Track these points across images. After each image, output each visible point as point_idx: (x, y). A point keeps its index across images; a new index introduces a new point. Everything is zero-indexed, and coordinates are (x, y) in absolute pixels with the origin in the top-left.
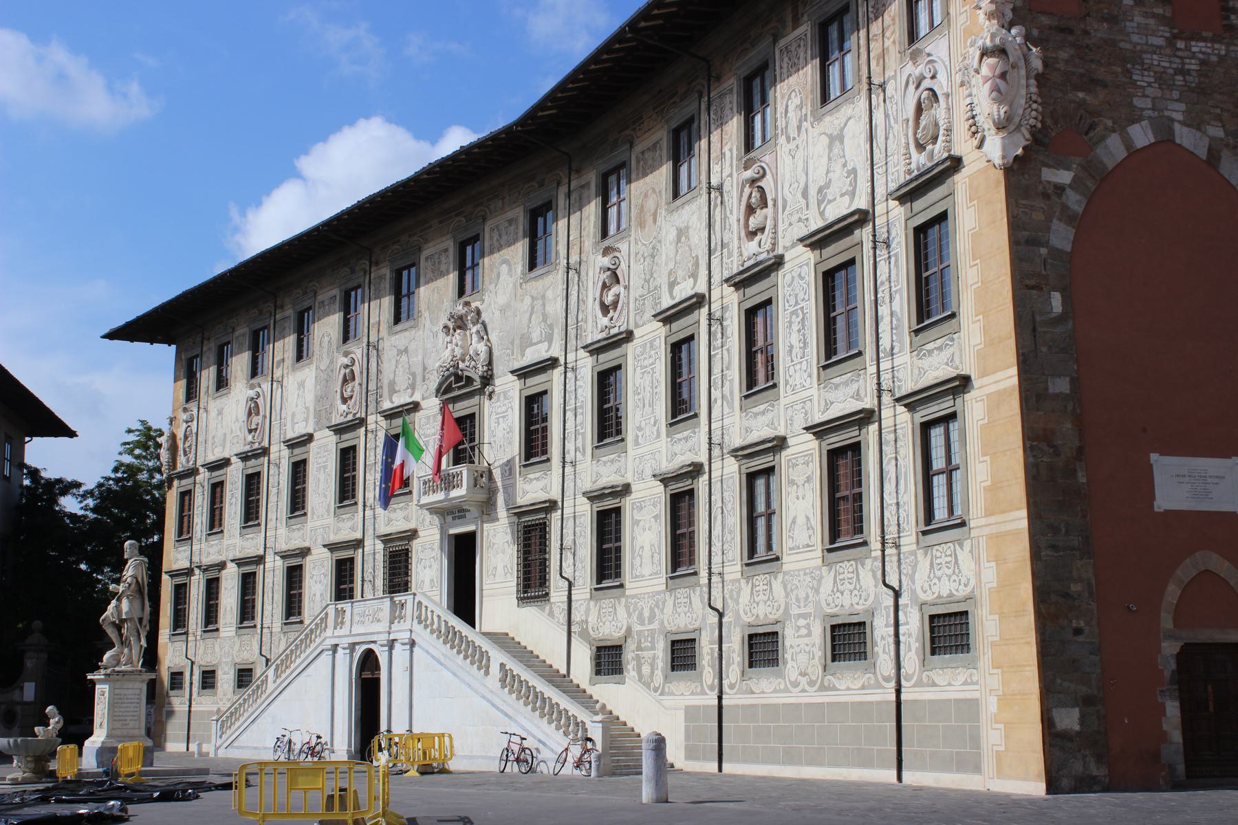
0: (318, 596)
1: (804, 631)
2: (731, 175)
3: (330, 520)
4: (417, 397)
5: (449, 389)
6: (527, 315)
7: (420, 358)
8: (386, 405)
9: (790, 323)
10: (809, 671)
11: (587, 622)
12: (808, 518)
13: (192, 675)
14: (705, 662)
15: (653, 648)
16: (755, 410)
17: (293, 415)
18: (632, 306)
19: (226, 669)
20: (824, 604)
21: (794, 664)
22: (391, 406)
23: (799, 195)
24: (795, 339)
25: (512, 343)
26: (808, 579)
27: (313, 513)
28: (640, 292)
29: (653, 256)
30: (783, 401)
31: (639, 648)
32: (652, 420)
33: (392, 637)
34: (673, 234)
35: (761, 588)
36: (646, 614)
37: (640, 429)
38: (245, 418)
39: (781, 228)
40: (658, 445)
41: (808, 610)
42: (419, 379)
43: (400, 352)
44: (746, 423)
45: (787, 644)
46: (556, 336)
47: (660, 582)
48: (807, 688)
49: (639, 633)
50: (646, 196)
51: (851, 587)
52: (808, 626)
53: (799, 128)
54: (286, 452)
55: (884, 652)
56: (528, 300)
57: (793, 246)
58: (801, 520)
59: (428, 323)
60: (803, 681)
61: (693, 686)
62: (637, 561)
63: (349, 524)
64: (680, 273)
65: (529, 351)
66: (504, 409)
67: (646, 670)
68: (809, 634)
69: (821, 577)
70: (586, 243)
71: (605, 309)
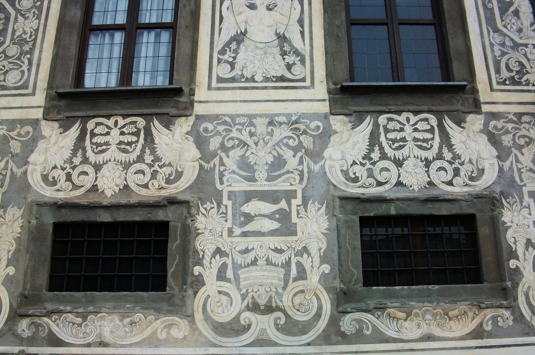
1: (275, 225)
10: (286, 302)
12: (282, 38)
20: (337, 178)
21: (226, 286)
35: (115, 136)
41: (281, 185)
45: (204, 244)
48: (274, 334)
51: (430, 155)
52: (284, 217)
60: (262, 324)
69: (325, 136)
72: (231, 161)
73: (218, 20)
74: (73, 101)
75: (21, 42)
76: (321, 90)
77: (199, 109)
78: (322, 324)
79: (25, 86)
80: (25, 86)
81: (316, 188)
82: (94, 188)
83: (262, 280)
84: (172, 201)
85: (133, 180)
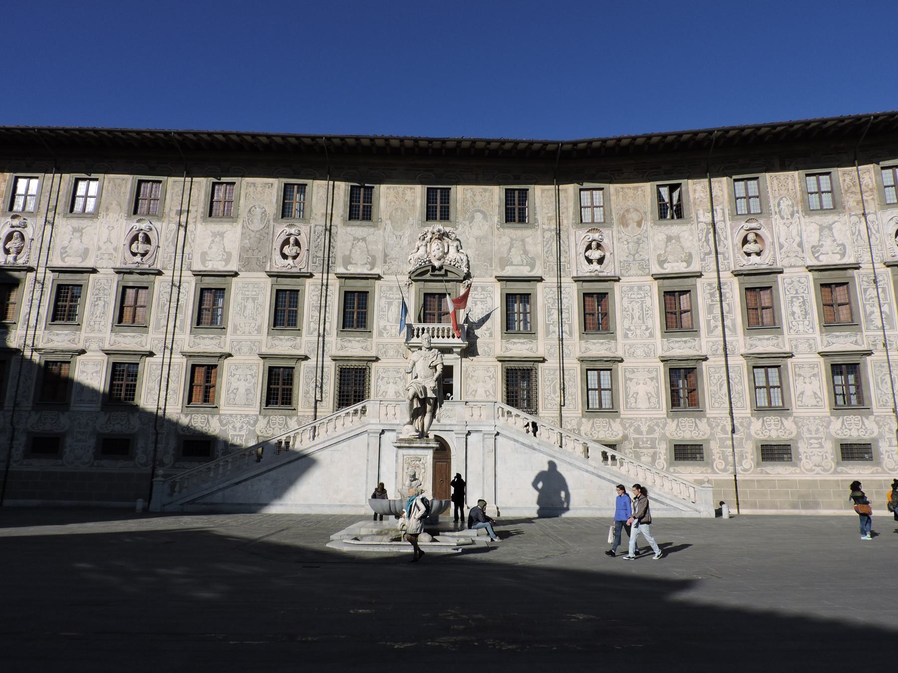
0: (242, 390)
2: (724, 221)
4: (376, 271)
5: (426, 272)
6: (507, 247)
7: (380, 247)
8: (341, 270)
9: (792, 302)
10: (823, 464)
11: (579, 430)
13: (12, 439)
17: (204, 255)
20: (834, 434)
22: (345, 271)
23: (795, 245)
24: (796, 309)
25: (491, 259)
26: (818, 421)
28: (625, 259)
29: (638, 242)
30: (786, 336)
31: (637, 445)
32: (644, 327)
33: (468, 428)
36: (644, 429)
37: (629, 329)
38: (127, 242)
39: (778, 257)
41: (819, 435)
42: (379, 261)
43: (355, 239)
44: (749, 341)
45: (801, 450)
50: (628, 211)
52: (820, 444)
53: (792, 215)
54: (193, 280)
55: (888, 457)
56: (506, 240)
57: (791, 266)
58: (808, 393)
59: (389, 227)
60: (818, 469)
61: (703, 469)
62: (632, 400)
63: (290, 343)
64: (670, 258)
65: (507, 268)
66: (482, 296)
68: (821, 446)
69: (829, 423)
71: (590, 261)
72: (805, 429)
73: (795, 387)
74: (759, 410)
75: (738, 393)
76: (827, 409)
77: (794, 414)
78: (832, 470)
81: (829, 436)
83: (817, 459)
84: (791, 440)
85: (780, 434)
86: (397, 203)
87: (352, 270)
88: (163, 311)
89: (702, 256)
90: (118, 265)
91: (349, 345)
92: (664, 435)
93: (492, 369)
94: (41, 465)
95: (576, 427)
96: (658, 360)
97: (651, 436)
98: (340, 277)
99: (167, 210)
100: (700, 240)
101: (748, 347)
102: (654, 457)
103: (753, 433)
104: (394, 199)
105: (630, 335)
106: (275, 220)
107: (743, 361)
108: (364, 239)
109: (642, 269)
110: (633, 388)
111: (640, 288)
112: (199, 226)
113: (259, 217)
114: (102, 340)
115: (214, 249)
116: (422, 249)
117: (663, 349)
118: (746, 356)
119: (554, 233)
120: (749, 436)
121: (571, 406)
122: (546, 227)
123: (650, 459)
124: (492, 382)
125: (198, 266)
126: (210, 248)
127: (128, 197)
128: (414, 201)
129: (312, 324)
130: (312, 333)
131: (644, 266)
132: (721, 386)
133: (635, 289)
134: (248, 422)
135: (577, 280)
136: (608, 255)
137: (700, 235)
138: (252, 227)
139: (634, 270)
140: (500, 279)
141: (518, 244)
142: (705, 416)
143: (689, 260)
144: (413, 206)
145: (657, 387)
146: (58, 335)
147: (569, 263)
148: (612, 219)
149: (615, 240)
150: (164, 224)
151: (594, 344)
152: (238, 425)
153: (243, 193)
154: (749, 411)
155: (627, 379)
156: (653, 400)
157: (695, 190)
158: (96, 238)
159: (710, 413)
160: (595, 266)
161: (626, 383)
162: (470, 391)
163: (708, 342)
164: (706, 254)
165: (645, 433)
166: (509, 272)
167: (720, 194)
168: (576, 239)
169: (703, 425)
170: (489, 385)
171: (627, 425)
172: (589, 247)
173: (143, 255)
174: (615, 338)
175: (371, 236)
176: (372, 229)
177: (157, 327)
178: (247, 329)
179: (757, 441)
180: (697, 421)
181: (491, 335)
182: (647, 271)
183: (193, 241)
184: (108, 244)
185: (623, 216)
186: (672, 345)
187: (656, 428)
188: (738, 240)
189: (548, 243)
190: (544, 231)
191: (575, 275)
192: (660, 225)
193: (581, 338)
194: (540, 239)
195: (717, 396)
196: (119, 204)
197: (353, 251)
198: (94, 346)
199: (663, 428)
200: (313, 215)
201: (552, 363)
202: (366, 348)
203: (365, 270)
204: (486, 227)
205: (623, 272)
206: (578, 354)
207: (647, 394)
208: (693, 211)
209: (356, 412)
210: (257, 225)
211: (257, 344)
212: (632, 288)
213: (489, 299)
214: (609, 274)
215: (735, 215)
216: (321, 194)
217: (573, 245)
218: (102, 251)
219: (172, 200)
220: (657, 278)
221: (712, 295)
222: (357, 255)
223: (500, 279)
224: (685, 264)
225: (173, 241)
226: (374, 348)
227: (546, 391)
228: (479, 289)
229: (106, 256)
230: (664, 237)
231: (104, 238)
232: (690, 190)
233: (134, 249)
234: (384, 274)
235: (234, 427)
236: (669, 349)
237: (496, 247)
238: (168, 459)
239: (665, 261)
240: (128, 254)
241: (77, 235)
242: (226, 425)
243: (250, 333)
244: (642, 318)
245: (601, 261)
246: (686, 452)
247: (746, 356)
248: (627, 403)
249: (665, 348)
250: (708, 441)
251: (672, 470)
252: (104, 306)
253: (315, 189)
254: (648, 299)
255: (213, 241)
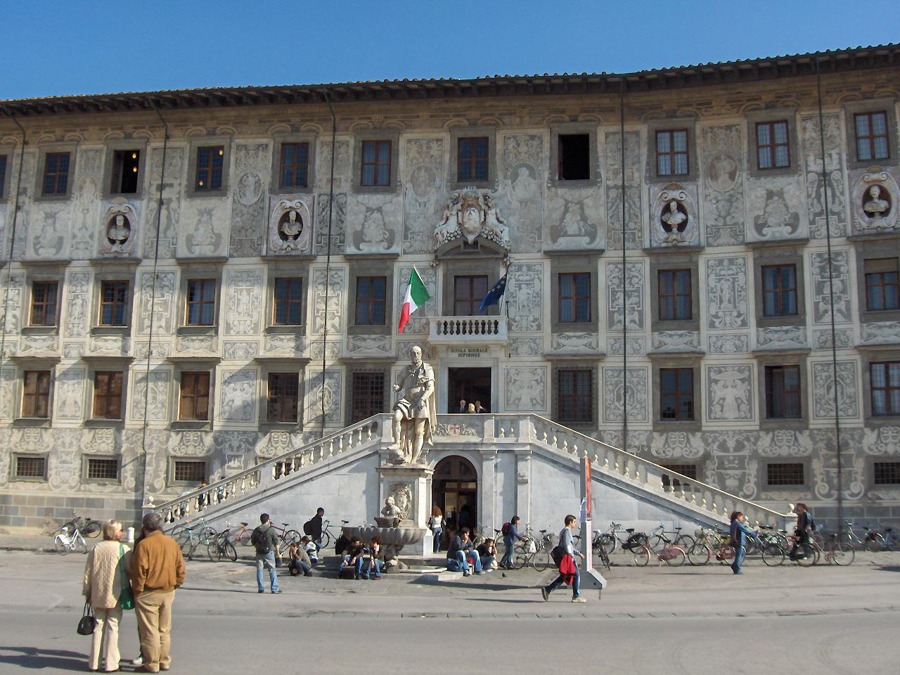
2: (841, 170)
3: (261, 337)
4: (396, 249)
7: (400, 218)
8: (351, 250)
11: (649, 447)
14: (818, 479)
15: (742, 466)
16: (880, 324)
18: (702, 230)
19: (64, 458)
25: (539, 229)
27: (228, 328)
28: (713, 223)
29: (730, 201)
31: (721, 465)
32: (735, 314)
34: (761, 192)
36: (731, 444)
37: (716, 316)
38: (104, 228)
40: (744, 331)
42: (399, 237)
43: (369, 209)
44: (868, 330)
46: (599, 234)
47: (754, 424)
49: (721, 459)
50: (718, 158)
59: (410, 193)
62: (717, 408)
64: (771, 220)
66: (528, 278)
67: (731, 483)
70: (636, 175)
71: (668, 228)
75: (850, 397)
79: (855, 415)
80: (855, 415)
82: (886, 452)
86: (421, 160)
87: (365, 249)
88: (146, 310)
89: (811, 218)
90: (95, 255)
91: (363, 344)
92: (755, 452)
93: (539, 371)
94: (28, 489)
95: (645, 443)
96: (751, 356)
97: (739, 454)
98: (349, 258)
99: (146, 184)
100: (809, 196)
101: (865, 336)
102: (742, 481)
103: (865, 449)
104: (417, 156)
105: (717, 324)
106: (272, 191)
107: (857, 358)
108: (379, 210)
109: (735, 235)
110: (719, 392)
111: (731, 261)
112: (184, 203)
113: (252, 188)
114: (82, 345)
115: (202, 230)
116: (453, 220)
117: (758, 342)
118: (860, 349)
119: (621, 190)
120: (860, 453)
121: (640, 417)
122: (610, 183)
123: (736, 483)
124: (540, 388)
125: (183, 252)
126: (196, 230)
127: (102, 172)
128: (441, 156)
129: (318, 320)
130: (317, 331)
131: (737, 231)
132: (829, 388)
133: (726, 263)
134: (247, 441)
135: (649, 252)
136: (690, 217)
137: (810, 189)
138: (244, 201)
139: (725, 236)
140: (548, 254)
141: (576, 208)
142: (807, 428)
143: (794, 223)
144: (441, 163)
145: (750, 391)
146: (35, 340)
147: (641, 230)
148: (698, 169)
149: (700, 197)
150: (145, 202)
151: (671, 336)
152: (235, 444)
153: (233, 159)
154: (861, 420)
155: (712, 381)
156: (743, 407)
157: (804, 129)
158: (70, 223)
159: (814, 423)
160: (675, 235)
161: (710, 387)
162: (512, 399)
163: (815, 331)
164: (816, 215)
165: (731, 450)
166: (563, 244)
167: (836, 133)
168: (650, 198)
169: (805, 441)
170: (536, 392)
171: (710, 440)
172: (667, 209)
173: (123, 242)
174: (698, 328)
175: (389, 205)
176: (389, 197)
177: (141, 329)
178: (242, 327)
179: (868, 458)
180: (797, 432)
181: (539, 327)
182: (741, 238)
183: (177, 222)
184: (84, 230)
185: (712, 166)
186: (770, 336)
187: (746, 443)
188: (858, 192)
189: (613, 204)
190: (608, 188)
191: (647, 245)
192: (758, 177)
193: (653, 330)
194: (603, 199)
195: (823, 402)
196: (93, 182)
197: (366, 226)
198: (74, 353)
199: (755, 444)
200: (317, 181)
201: (613, 362)
202: (383, 348)
203: (381, 249)
204: (534, 187)
205: (710, 240)
206: (649, 349)
207: (736, 399)
208: (801, 153)
209: (365, 429)
210: (251, 198)
211: (253, 346)
212: (720, 262)
213: (536, 281)
214: (691, 244)
215: (856, 161)
216: (325, 154)
217: (645, 206)
218: (78, 239)
219: (152, 172)
220: (756, 247)
221: (822, 269)
222: (373, 231)
223: (548, 254)
224: (789, 229)
225: (154, 223)
226: (394, 346)
227: (609, 398)
228: (524, 268)
229: (82, 246)
230: (764, 192)
231: (79, 225)
232: (799, 128)
233: (113, 237)
234: (405, 253)
235: (230, 446)
236: (766, 342)
237: (546, 213)
238: (160, 483)
239: (765, 225)
240: (106, 242)
241: (50, 221)
242: (221, 443)
243: (245, 332)
244: (733, 301)
245: (682, 227)
246: (784, 474)
247: (860, 349)
248: (710, 411)
249: (762, 340)
250: (809, 459)
251: (763, 495)
252: (82, 304)
253: (318, 148)
254: (741, 277)
255: (200, 221)
